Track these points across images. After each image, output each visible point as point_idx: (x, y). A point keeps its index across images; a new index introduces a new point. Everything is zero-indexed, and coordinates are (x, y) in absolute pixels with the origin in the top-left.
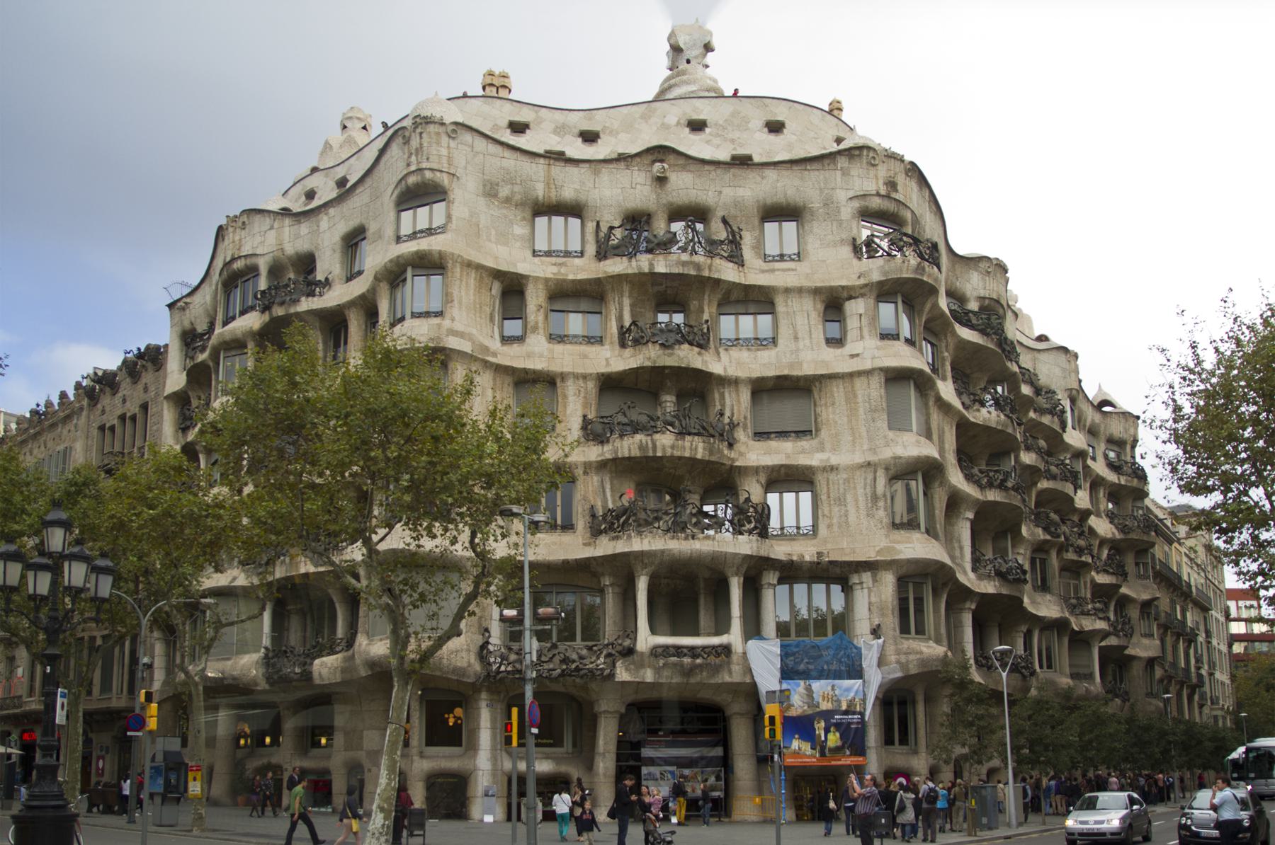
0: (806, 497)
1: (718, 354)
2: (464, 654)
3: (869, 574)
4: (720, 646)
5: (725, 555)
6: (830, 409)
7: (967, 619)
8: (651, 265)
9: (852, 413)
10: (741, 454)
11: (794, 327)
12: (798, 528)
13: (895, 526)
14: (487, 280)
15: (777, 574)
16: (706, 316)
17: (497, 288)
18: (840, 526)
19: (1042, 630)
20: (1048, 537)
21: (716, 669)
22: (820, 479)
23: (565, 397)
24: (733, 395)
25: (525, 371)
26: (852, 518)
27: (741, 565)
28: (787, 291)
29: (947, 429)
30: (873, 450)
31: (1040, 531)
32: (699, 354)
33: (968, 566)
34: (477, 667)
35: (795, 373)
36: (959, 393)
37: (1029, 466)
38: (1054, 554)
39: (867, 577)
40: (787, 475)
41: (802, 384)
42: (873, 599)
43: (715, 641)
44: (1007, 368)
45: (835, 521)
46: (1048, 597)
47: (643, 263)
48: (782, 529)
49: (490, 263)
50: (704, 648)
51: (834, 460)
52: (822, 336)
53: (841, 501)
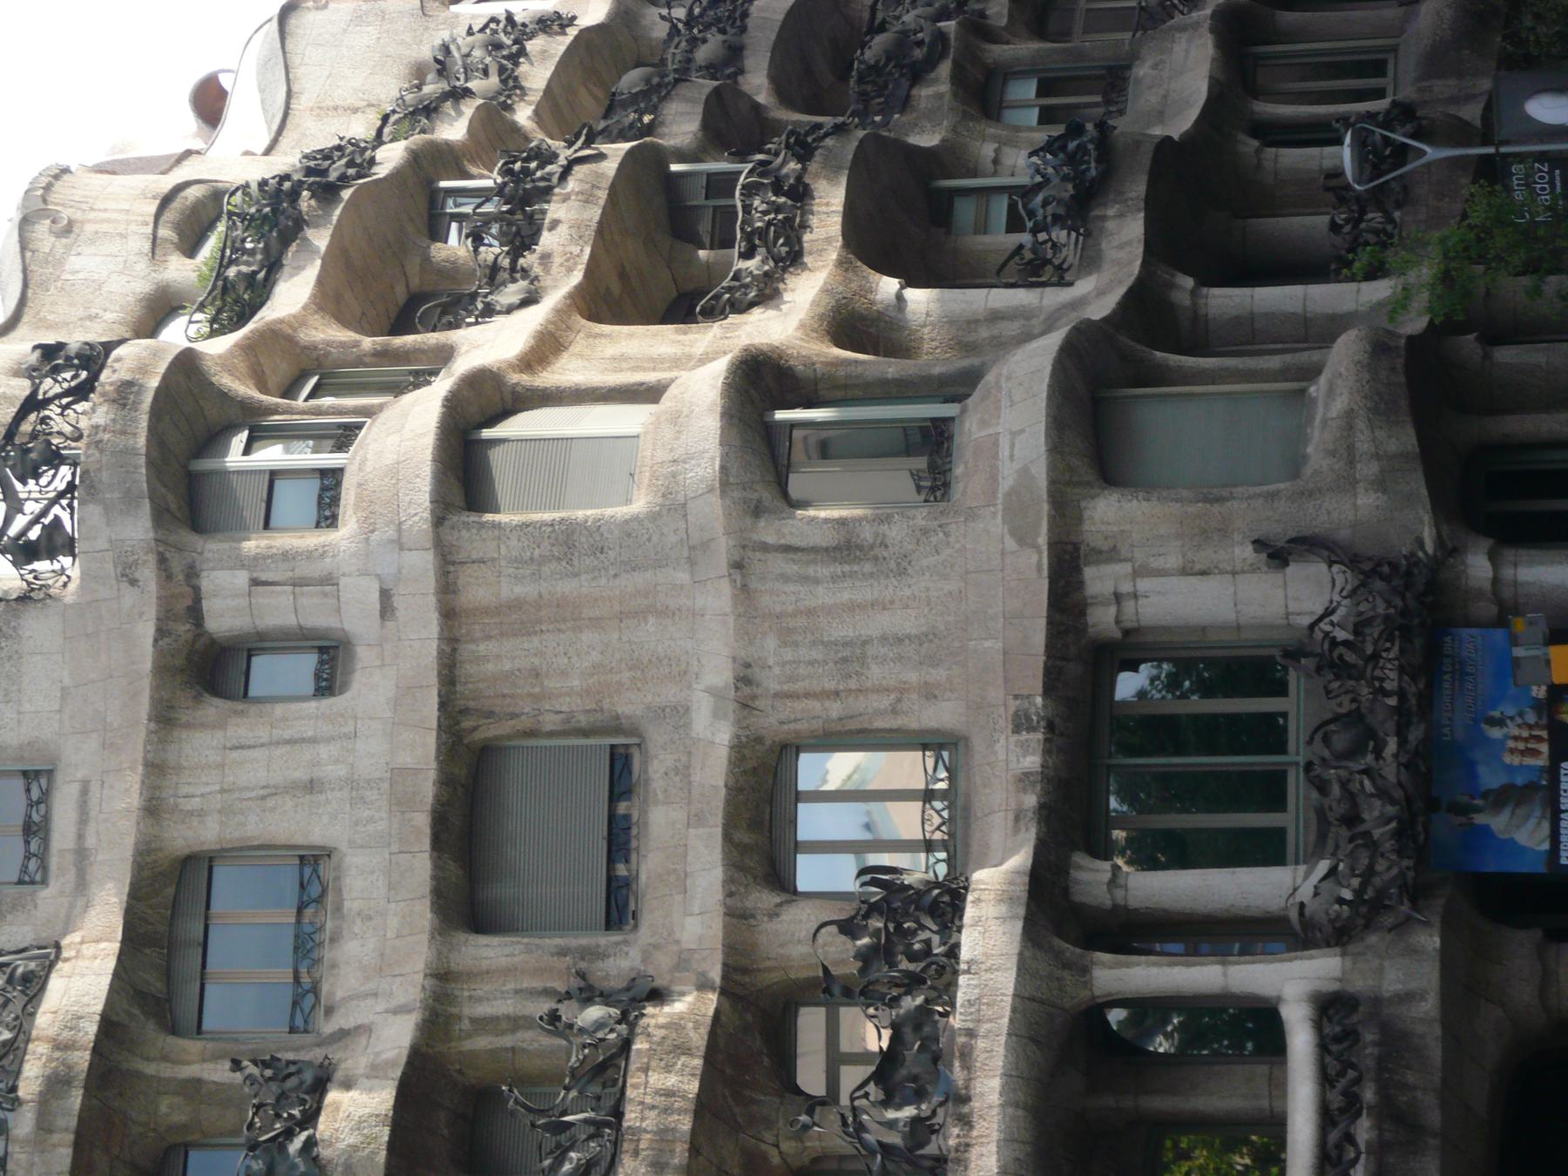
1: (343, 1035)
3: (1089, 573)
4: (1318, 1025)
5: (1022, 998)
6: (552, 684)
7: (1225, 301)
9: (567, 614)
11: (272, 792)
12: (928, 796)
13: (937, 486)
15: (1080, 858)
16: (220, 1073)
18: (932, 661)
19: (1256, 93)
20: (945, 69)
21: (1396, 1042)
22: (774, 721)
24: (482, 989)
26: (905, 622)
27: (1057, 954)
28: (153, 809)
29: (611, 350)
30: (695, 552)
31: (924, 94)
33: (1054, 297)
35: (427, 788)
36: (489, 311)
37: (706, 125)
38: (998, 52)
39: (1099, 580)
40: (755, 825)
42: (1173, 561)
43: (1301, 1041)
44: (396, 175)
45: (913, 677)
46: (1142, 70)
50: (1325, 1079)
51: (717, 673)
52: (312, 706)
53: (851, 656)
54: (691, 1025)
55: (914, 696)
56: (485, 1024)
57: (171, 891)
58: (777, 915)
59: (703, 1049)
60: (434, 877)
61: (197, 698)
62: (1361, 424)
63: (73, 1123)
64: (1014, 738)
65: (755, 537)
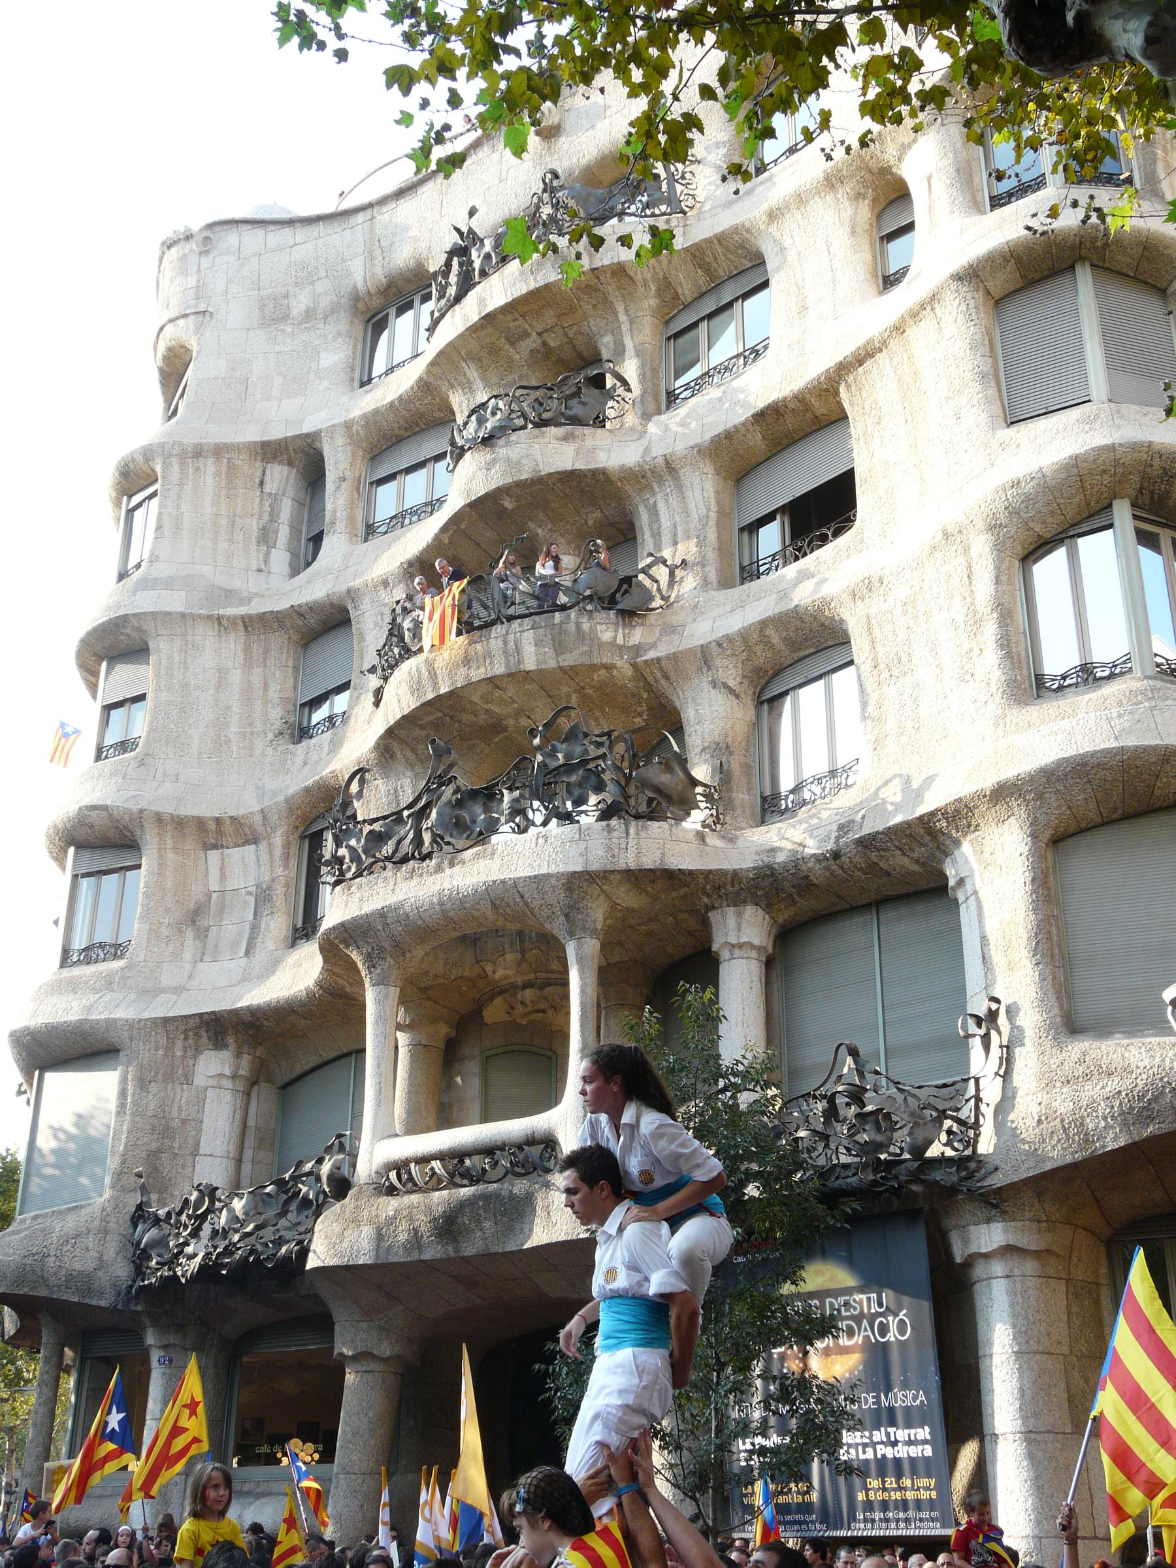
0: (843, 680)
2: (91, 1242)
4: (531, 1140)
8: (481, 302)
10: (670, 629)
14: (250, 469)
17: (279, 477)
23: (362, 637)
25: (298, 612)
28: (773, 215)
32: (565, 438)
34: (122, 1271)
40: (793, 645)
41: (819, 408)
47: (470, 310)
48: (797, 789)
49: (253, 434)
50: (489, 1150)
54: (586, 648)
55: (876, 732)
56: (654, 512)
57: (750, 265)
58: (714, 687)
59: (566, 663)
60: (735, 427)
61: (858, 196)
62: (1113, 1085)
63: (541, 283)
64: (834, 827)
65: (971, 536)
